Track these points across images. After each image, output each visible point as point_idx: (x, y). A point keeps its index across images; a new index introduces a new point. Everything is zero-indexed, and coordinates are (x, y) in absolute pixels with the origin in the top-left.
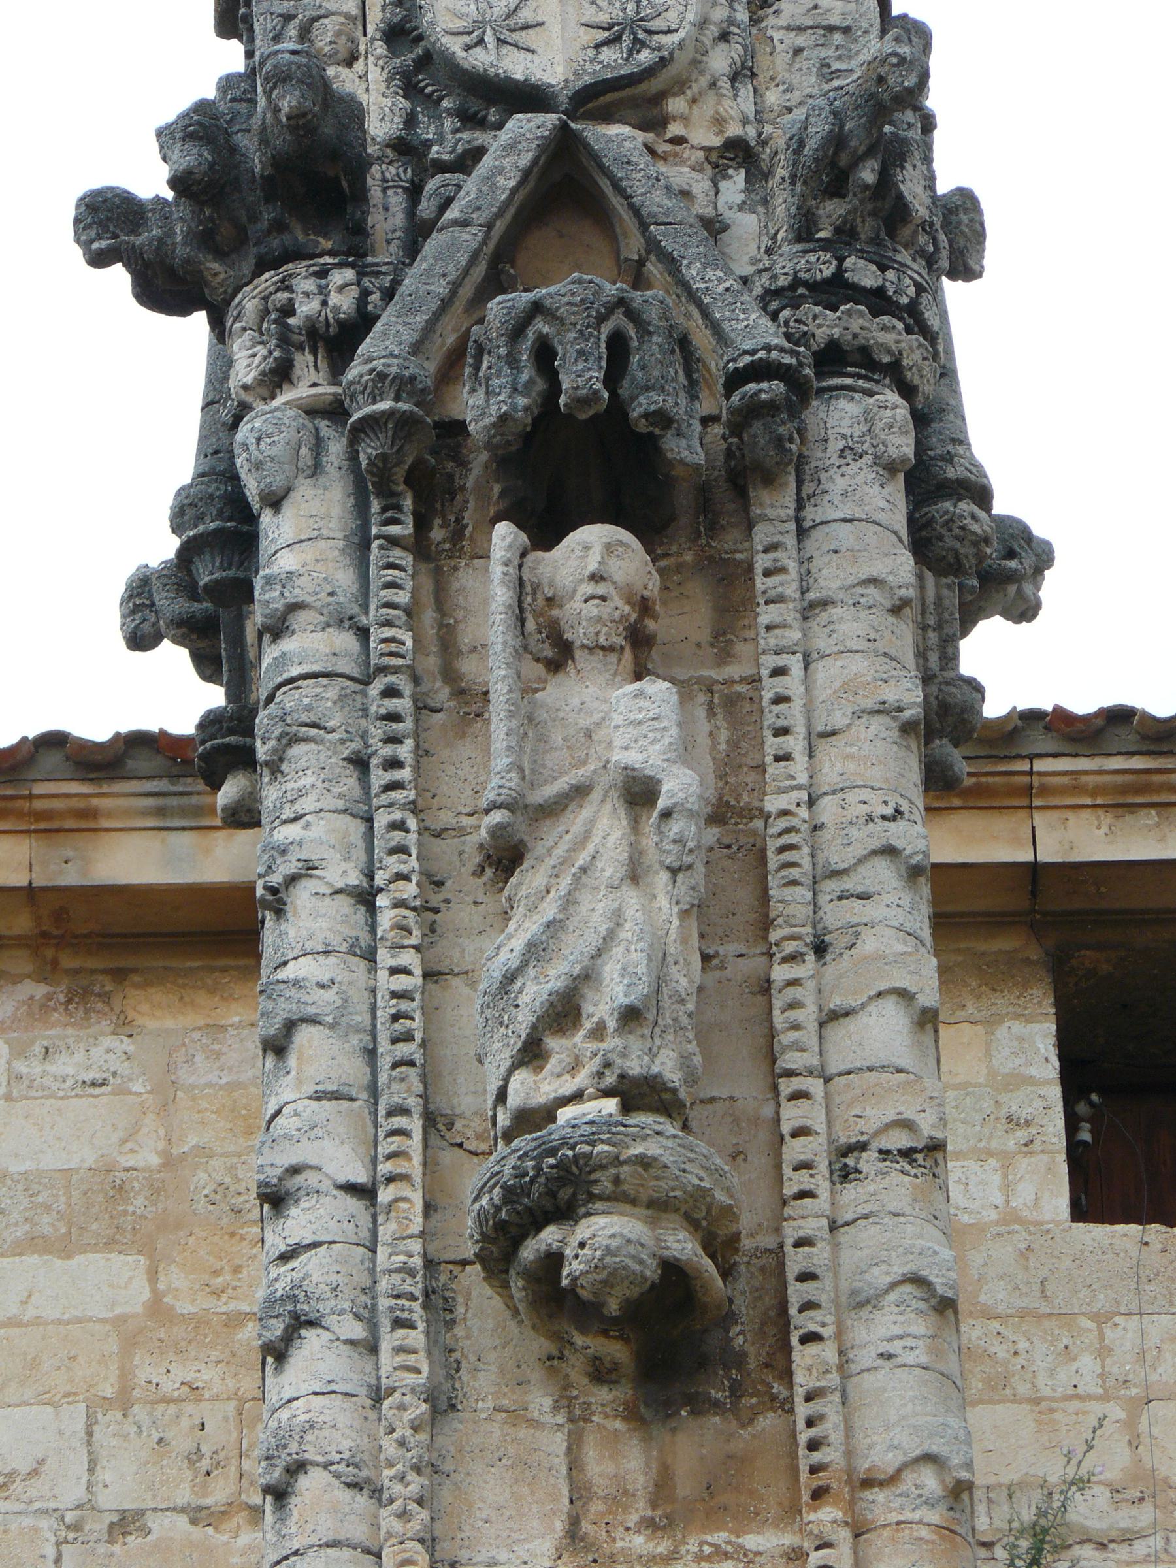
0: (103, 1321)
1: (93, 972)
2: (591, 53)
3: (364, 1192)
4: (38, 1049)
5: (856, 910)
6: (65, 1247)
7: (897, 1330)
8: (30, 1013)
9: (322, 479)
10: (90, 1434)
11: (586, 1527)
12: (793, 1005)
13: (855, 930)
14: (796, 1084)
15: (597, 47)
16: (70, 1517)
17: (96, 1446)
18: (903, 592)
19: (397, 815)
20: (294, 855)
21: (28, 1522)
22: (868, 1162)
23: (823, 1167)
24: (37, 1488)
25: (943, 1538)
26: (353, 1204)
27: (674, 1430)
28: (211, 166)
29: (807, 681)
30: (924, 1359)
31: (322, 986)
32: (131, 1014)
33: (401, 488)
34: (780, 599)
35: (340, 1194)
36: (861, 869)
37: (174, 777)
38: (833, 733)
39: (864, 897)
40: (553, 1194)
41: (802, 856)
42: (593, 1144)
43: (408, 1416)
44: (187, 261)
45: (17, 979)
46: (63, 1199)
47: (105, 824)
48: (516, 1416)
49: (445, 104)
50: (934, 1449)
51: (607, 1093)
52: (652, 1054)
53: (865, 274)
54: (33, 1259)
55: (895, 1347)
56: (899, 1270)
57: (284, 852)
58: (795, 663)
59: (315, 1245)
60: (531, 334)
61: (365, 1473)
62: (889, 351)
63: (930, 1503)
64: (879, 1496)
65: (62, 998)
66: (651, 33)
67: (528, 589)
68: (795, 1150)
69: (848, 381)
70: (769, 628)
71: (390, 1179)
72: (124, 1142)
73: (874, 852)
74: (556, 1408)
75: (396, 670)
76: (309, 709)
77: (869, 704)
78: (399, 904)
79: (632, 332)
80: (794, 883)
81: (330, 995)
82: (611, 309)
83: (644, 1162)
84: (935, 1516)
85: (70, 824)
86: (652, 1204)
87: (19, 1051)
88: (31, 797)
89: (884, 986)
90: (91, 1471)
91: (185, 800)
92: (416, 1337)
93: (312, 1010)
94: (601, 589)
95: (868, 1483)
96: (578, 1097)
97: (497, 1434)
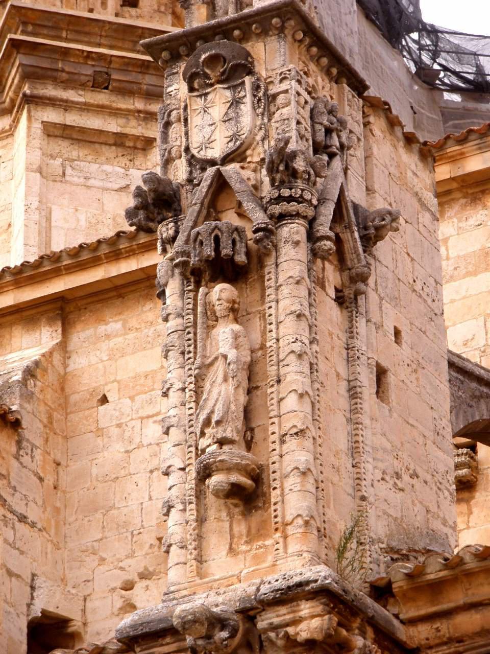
0: (486, 292)
1: (477, 192)
2: (226, 145)
3: (183, 469)
4: (464, 219)
5: (287, 369)
6: (475, 273)
7: (293, 483)
8: (462, 209)
9: (174, 278)
10: (485, 325)
11: (234, 546)
12: (272, 399)
13: (285, 375)
14: (272, 420)
15: (228, 143)
16: (482, 349)
17: (487, 328)
18: (297, 279)
19: (190, 367)
20: (169, 382)
21: (472, 352)
22: (287, 438)
23: (277, 441)
24: (474, 343)
25: (303, 535)
26: (181, 473)
27: (252, 516)
28: (142, 203)
29: (277, 309)
30: (299, 489)
31: (174, 416)
32: (486, 203)
33: (190, 276)
34: (270, 287)
35: (179, 471)
36: (287, 358)
37: (481, 138)
38: (281, 322)
39: (288, 365)
40: (205, 472)
41: (274, 358)
42: (209, 459)
43: (192, 527)
44: (145, 225)
45: (458, 199)
46: (474, 260)
47: (467, 155)
48: (219, 519)
49: (197, 167)
50: (300, 513)
51: (216, 443)
52: (225, 431)
53: (286, 192)
54: (467, 279)
55: (292, 487)
56: (293, 467)
57: (166, 382)
58: (273, 304)
59: (174, 486)
60: (198, 240)
61: (183, 544)
62: (295, 211)
63: (300, 527)
64: (289, 527)
65: (470, 202)
66: (239, 136)
67: (208, 304)
68: (272, 438)
69: (286, 222)
70: (268, 296)
71: (189, 465)
72: (487, 240)
73: (289, 353)
74: (227, 516)
75: (190, 327)
76: (171, 342)
77: (289, 312)
78: (191, 390)
79: (220, 234)
80: (272, 365)
81: (176, 419)
82: (213, 230)
83: (220, 461)
84: (301, 530)
85: (459, 157)
86: (227, 469)
87: (460, 221)
88: (447, 153)
89: (291, 390)
90: (486, 335)
91: (485, 144)
92: (193, 506)
93: (172, 423)
94: (220, 302)
95: (287, 525)
96: (209, 445)
97: (215, 525)
